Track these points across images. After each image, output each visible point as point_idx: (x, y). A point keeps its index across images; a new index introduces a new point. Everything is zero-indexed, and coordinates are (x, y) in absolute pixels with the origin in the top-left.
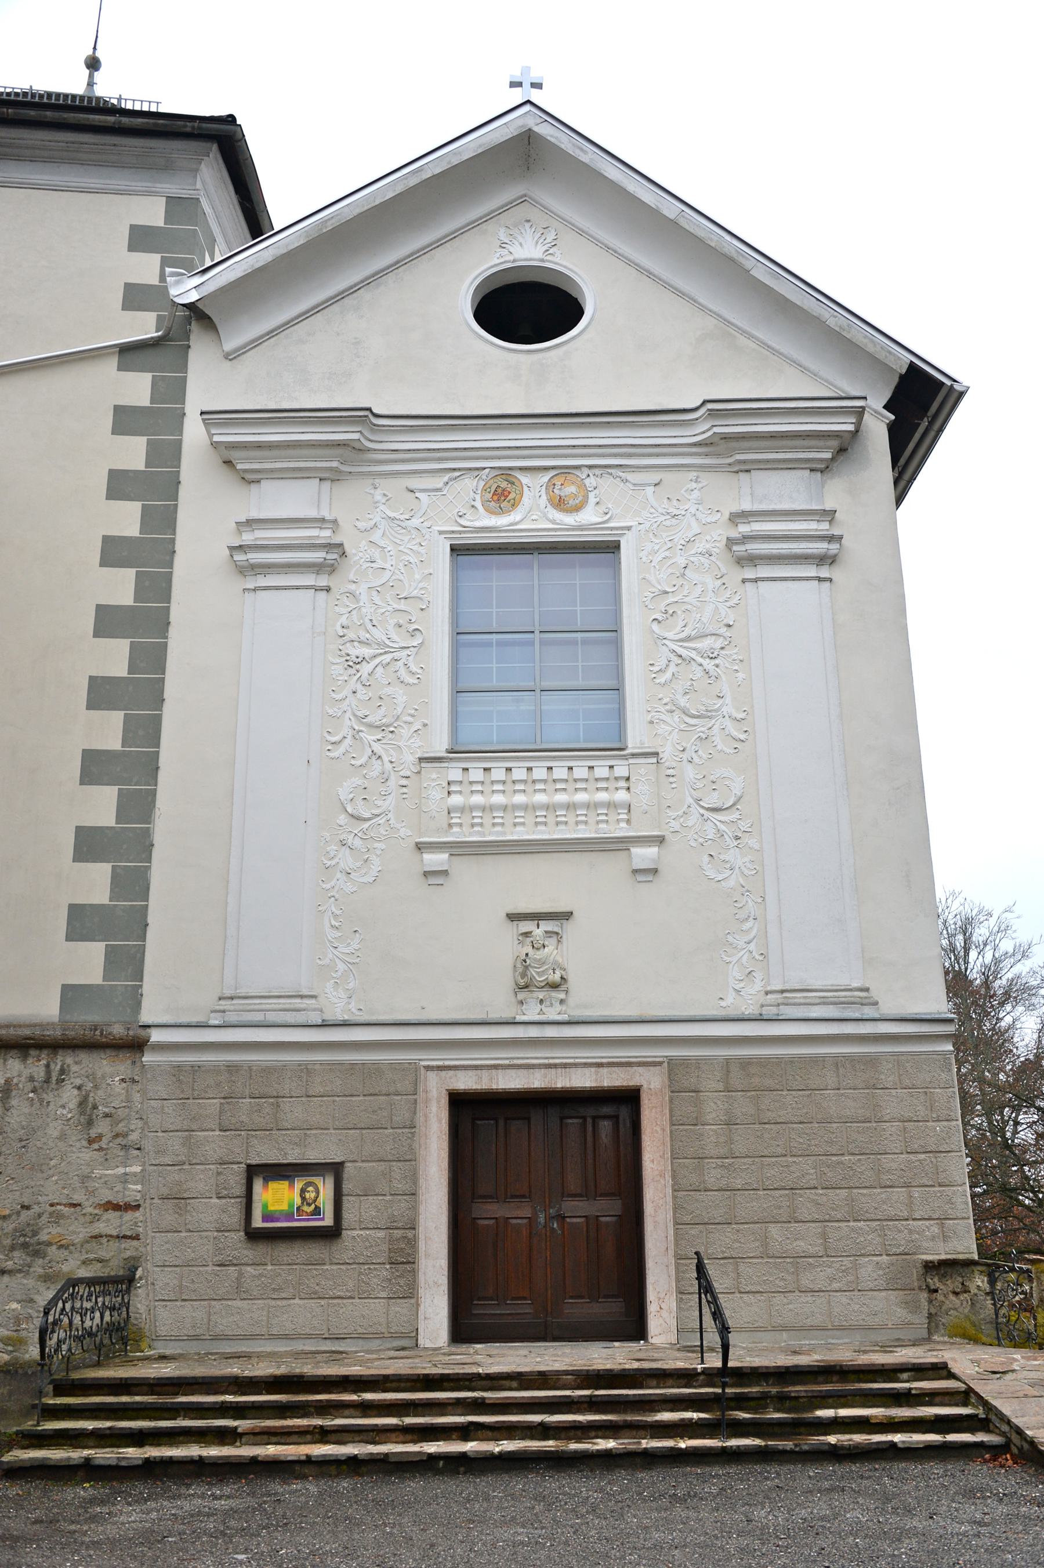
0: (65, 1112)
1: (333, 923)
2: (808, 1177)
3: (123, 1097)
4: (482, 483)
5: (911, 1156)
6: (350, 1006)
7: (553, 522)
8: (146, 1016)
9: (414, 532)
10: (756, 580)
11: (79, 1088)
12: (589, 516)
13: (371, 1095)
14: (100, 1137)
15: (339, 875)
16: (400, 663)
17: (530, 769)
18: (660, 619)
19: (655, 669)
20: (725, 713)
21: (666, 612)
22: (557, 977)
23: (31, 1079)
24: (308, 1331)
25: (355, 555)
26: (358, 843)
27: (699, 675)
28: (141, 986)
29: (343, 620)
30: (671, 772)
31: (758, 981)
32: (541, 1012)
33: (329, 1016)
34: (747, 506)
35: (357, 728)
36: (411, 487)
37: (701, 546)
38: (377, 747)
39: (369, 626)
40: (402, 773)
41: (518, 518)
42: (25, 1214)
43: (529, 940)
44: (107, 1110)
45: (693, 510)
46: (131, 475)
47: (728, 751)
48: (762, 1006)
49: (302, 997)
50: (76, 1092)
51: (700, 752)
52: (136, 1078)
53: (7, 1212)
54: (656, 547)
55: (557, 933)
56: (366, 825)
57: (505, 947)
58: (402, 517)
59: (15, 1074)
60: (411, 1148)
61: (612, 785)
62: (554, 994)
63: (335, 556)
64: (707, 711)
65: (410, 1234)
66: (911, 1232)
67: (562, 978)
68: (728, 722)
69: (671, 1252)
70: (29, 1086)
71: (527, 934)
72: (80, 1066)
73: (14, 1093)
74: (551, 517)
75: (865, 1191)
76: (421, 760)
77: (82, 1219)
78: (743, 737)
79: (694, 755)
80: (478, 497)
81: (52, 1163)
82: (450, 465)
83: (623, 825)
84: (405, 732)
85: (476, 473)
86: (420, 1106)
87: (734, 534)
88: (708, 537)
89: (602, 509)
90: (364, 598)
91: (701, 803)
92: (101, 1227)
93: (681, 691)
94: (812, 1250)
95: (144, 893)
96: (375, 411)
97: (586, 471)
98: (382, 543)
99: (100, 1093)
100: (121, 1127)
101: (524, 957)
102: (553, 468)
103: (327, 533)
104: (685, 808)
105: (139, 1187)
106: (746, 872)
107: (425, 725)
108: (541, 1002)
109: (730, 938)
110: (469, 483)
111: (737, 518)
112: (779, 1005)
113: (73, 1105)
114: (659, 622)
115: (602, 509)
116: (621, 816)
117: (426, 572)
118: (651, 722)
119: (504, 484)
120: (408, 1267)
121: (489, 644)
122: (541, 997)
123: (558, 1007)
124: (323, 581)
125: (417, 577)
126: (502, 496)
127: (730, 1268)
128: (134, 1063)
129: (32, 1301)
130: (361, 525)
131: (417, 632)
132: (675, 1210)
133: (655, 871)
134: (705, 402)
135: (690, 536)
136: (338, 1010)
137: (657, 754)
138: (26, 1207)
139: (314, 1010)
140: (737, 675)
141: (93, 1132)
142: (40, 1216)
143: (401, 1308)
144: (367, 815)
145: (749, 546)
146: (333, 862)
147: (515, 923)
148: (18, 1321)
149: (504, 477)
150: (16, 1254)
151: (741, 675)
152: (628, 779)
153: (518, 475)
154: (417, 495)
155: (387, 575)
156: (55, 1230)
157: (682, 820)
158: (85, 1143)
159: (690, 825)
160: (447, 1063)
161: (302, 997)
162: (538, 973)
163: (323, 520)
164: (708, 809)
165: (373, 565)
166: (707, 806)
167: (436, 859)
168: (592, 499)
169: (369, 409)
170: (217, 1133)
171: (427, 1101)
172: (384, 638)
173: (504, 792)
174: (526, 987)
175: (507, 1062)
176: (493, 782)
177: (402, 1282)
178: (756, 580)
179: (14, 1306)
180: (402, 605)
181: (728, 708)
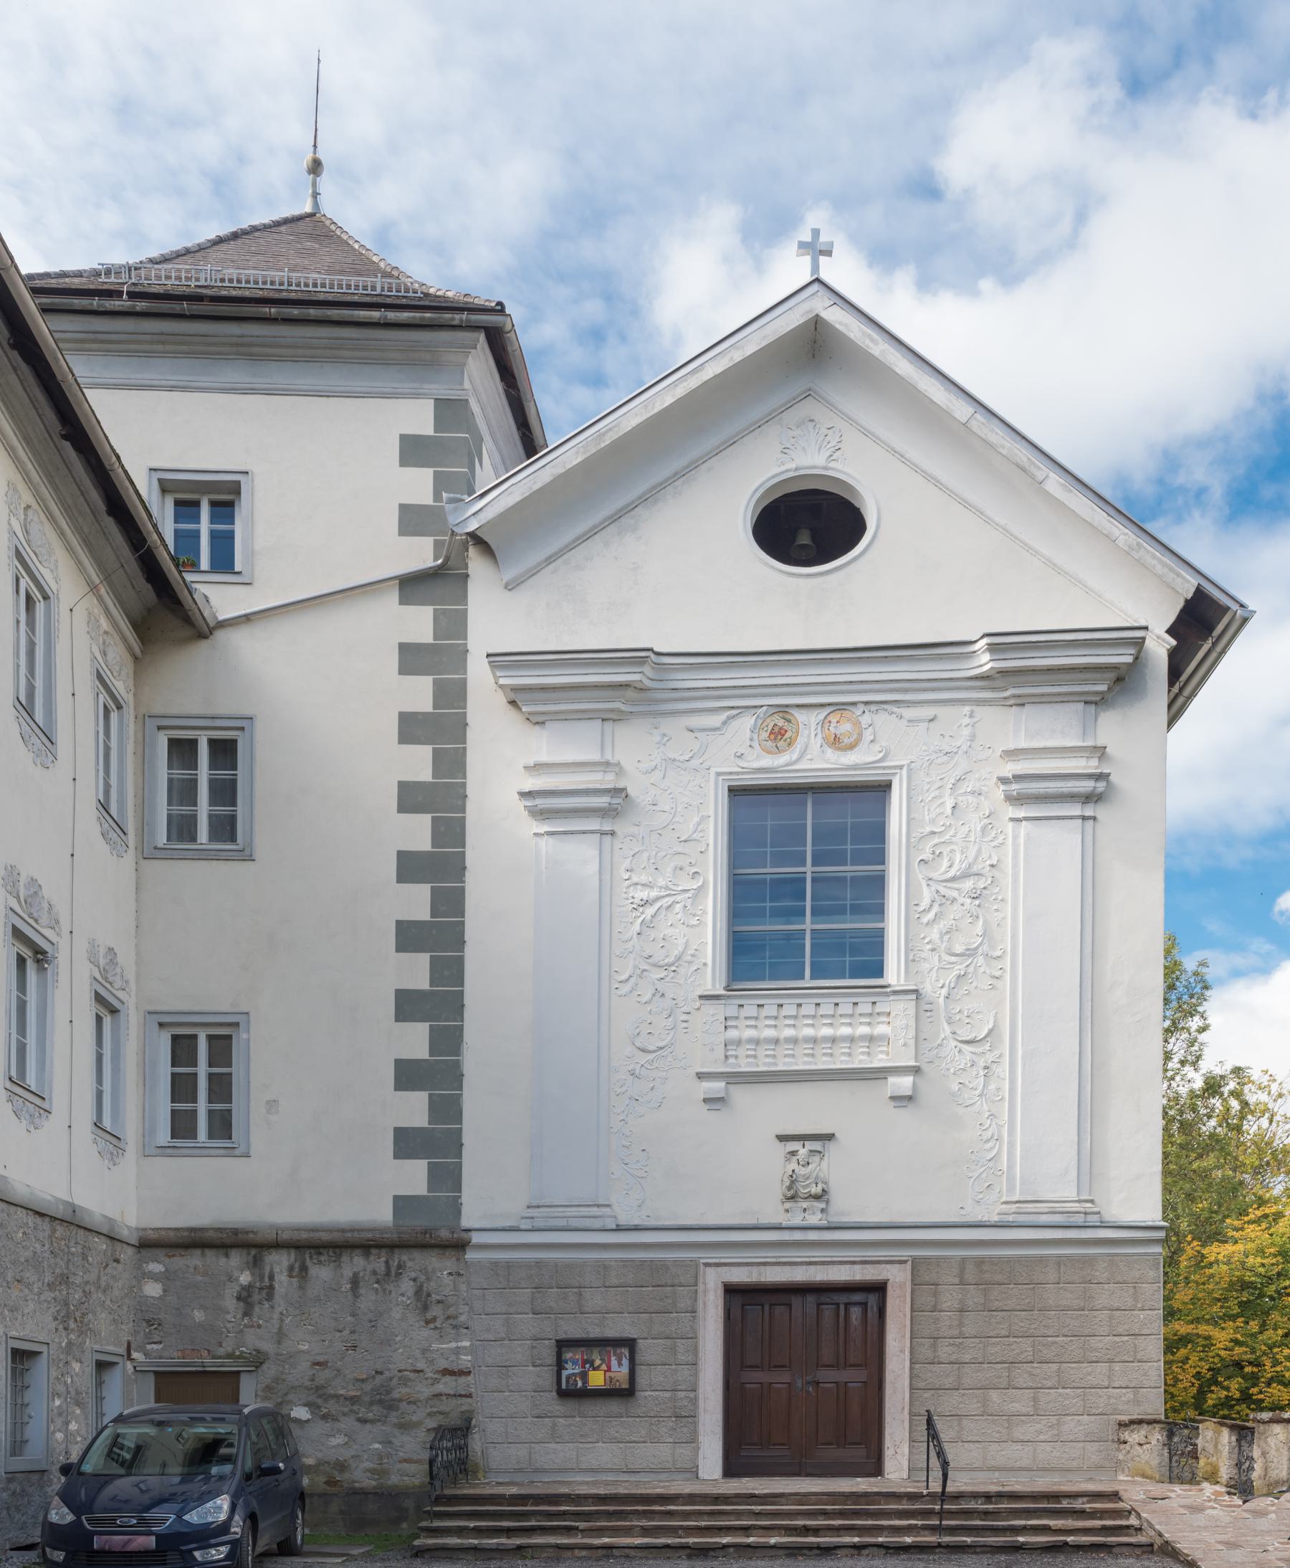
5: (1117, 1339)
8: (465, 1223)
11: (414, 1280)
14: (434, 1319)
17: (799, 1005)
23: (374, 1273)
38: (660, 986)
42: (378, 1378)
43: (795, 1158)
49: (598, 1206)
53: (365, 1376)
56: (651, 1056)
60: (694, 1330)
65: (692, 1395)
66: (1109, 1397)
69: (907, 1410)
70: (373, 1278)
71: (793, 1153)
72: (415, 1261)
76: (701, 997)
81: (398, 1339)
86: (700, 1295)
92: (440, 1388)
94: (1024, 1410)
95: (458, 1117)
99: (432, 1284)
100: (451, 1311)
105: (469, 1358)
113: (411, 1292)
123: (819, 1215)
127: (955, 1423)
128: (458, 1260)
129: (390, 1442)
132: (911, 1378)
138: (381, 1373)
141: (429, 1315)
142: (391, 1379)
144: (652, 1048)
146: (623, 1089)
148: (381, 1458)
150: (375, 1408)
156: (404, 1390)
158: (423, 1323)
160: (723, 1261)
161: (598, 1206)
167: (717, 1087)
171: (705, 1291)
177: (685, 1430)
179: (377, 1446)
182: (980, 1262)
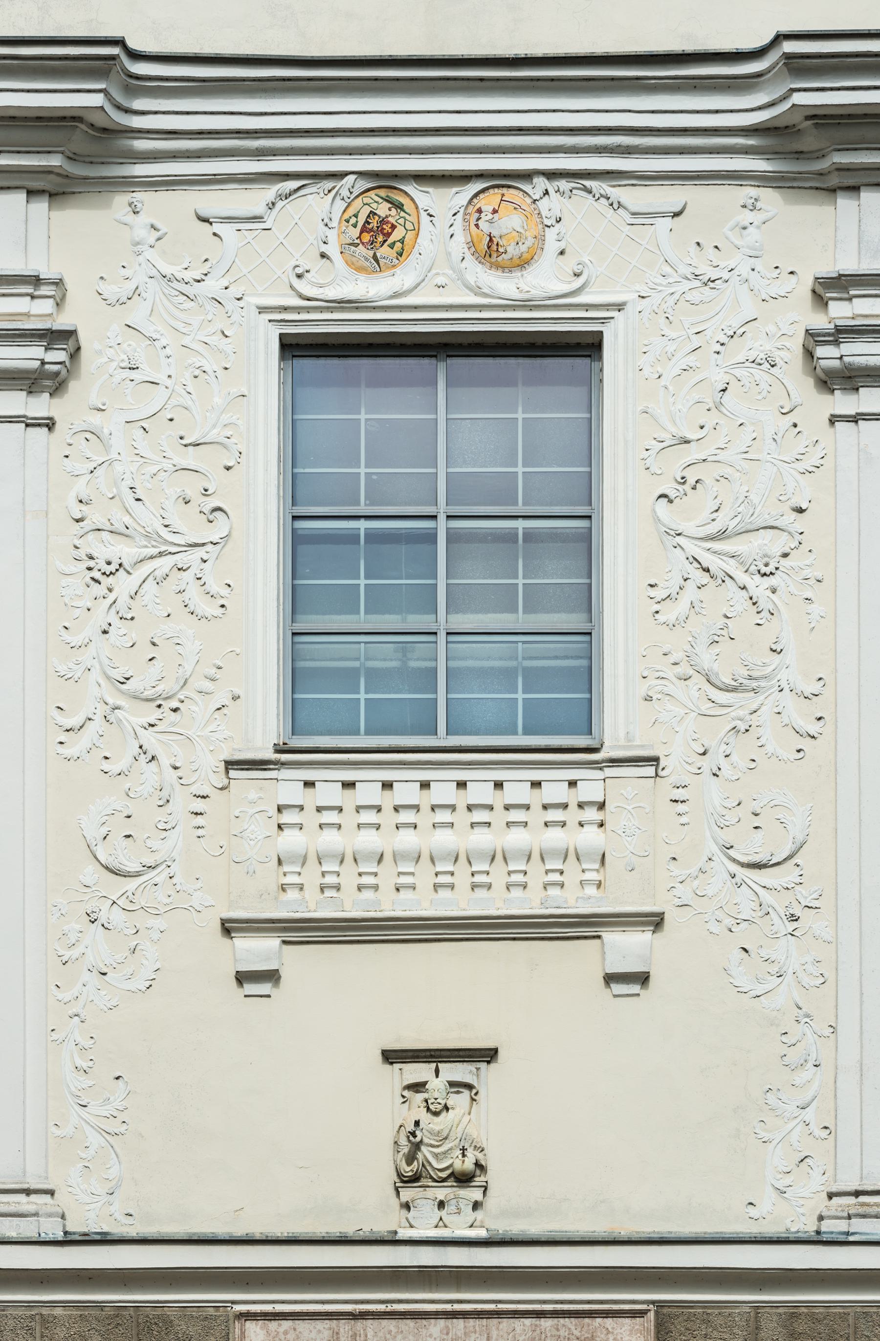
1: (79, 1063)
4: (340, 205)
6: (112, 1209)
7: (477, 291)
9: (211, 306)
10: (855, 419)
12: (544, 280)
15: (86, 976)
16: (188, 576)
17: (425, 785)
18: (672, 494)
19: (659, 593)
20: (784, 684)
21: (683, 481)
22: (469, 1165)
25: (99, 353)
26: (116, 917)
27: (739, 608)
29: (81, 488)
30: (679, 794)
31: (816, 1174)
32: (441, 1223)
33: (76, 1226)
34: (849, 265)
35: (110, 701)
36: (204, 213)
37: (757, 345)
38: (149, 738)
39: (129, 498)
41: (408, 284)
43: (420, 1097)
45: (744, 270)
47: (784, 755)
48: (821, 1218)
49: (28, 1192)
51: (734, 758)
54: (671, 348)
55: (469, 1087)
56: (131, 884)
57: (381, 1106)
58: (188, 276)
61: (573, 815)
62: (463, 1192)
63: (61, 356)
64: (750, 678)
67: (478, 1165)
68: (788, 701)
71: (418, 1087)
74: (471, 280)
76: (230, 765)
78: (813, 728)
79: (723, 763)
80: (332, 236)
82: (279, 162)
83: (591, 890)
84: (198, 710)
85: (328, 184)
87: (821, 322)
88: (771, 328)
89: (569, 264)
90: (118, 444)
91: (731, 852)
93: (704, 640)
96: (132, 44)
97: (541, 183)
98: (150, 331)
101: (411, 1127)
102: (481, 175)
103: (45, 306)
104: (701, 862)
106: (806, 980)
107: (235, 698)
108: (441, 1205)
109: (771, 1098)
110: (316, 204)
111: (832, 287)
112: (849, 1217)
114: (671, 501)
115: (569, 264)
116: (588, 876)
117: (235, 391)
118: (648, 699)
119: (383, 209)
121: (352, 538)
122: (441, 1197)
123: (469, 1215)
124: (39, 406)
125: (217, 400)
126: (376, 236)
130: (111, 290)
131: (218, 514)
133: (643, 979)
134: (779, 38)
135: (736, 324)
136: (92, 1215)
137: (656, 759)
139: (50, 1215)
140: (810, 608)
145: (846, 348)
146: (75, 953)
147: (397, 1066)
149: (383, 193)
151: (816, 609)
152: (602, 806)
153: (411, 188)
154: (217, 228)
155: (159, 397)
157: (696, 883)
159: (710, 893)
160: (279, 1308)
161: (28, 1192)
162: (436, 1156)
163: (36, 281)
164: (743, 865)
165: (133, 374)
166: (744, 859)
167: (258, 950)
168: (552, 246)
169: (119, 42)
172: (158, 526)
173: (378, 827)
174: (415, 1178)
175: (381, 1307)
176: (358, 809)
178: (855, 419)
180: (190, 458)
181: (792, 671)
182: (793, 1313)
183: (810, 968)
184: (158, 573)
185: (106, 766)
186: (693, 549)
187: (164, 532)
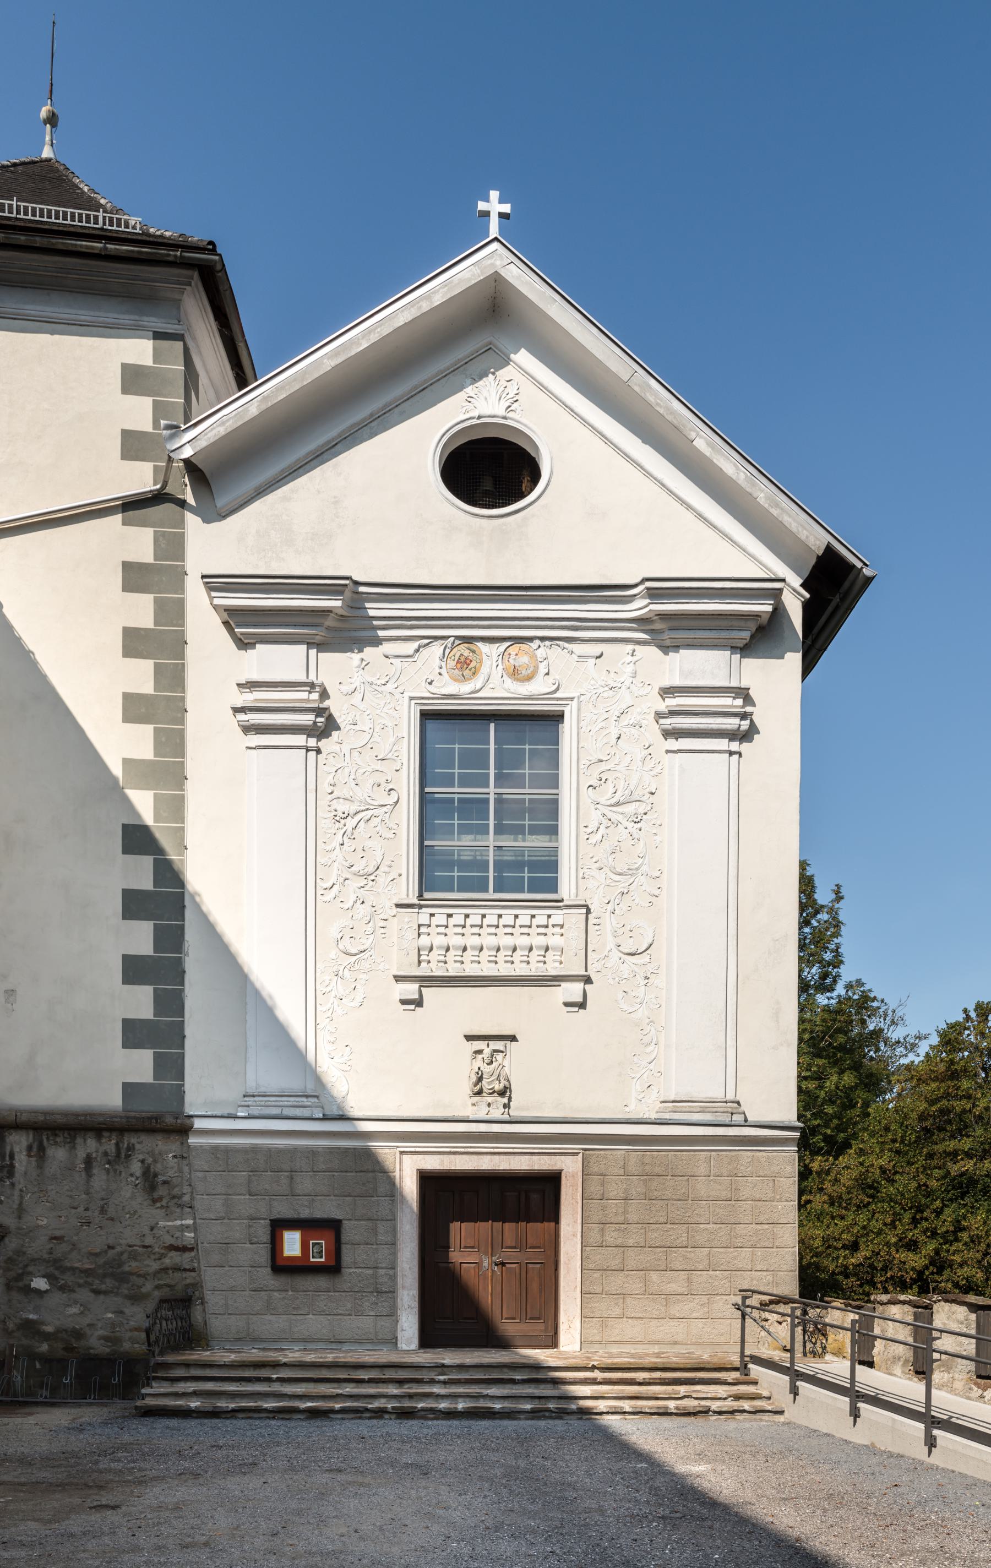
0: (133, 1179)
2: (681, 1239)
3: (176, 1169)
5: (758, 1226)
7: (508, 691)
8: (189, 1110)
9: (388, 696)
11: (143, 1161)
12: (538, 686)
13: (361, 1172)
19: (589, 830)
23: (106, 1154)
24: (319, 1336)
27: (624, 837)
28: (183, 1085)
36: (387, 654)
40: (382, 916)
41: (478, 687)
44: (164, 1178)
45: (627, 683)
46: (142, 632)
49: (307, 1096)
50: (139, 1164)
52: (185, 1155)
58: (379, 682)
59: (93, 1150)
65: (391, 1272)
71: (479, 1052)
72: (144, 1144)
73: (94, 1164)
75: (722, 1250)
76: (397, 906)
77: (153, 1257)
78: (657, 892)
94: (680, 1290)
95: (181, 1011)
97: (537, 642)
100: (176, 1191)
105: (192, 1235)
110: (436, 649)
111: (667, 692)
113: (138, 1173)
115: (550, 679)
119: (466, 653)
120: (390, 1295)
126: (466, 667)
128: (182, 1143)
141: (156, 1195)
143: (385, 1323)
144: (354, 951)
146: (328, 989)
149: (466, 645)
153: (480, 644)
154: (392, 660)
158: (149, 1202)
160: (418, 1150)
165: (354, 727)
168: (542, 669)
170: (247, 1197)
175: (463, 1150)
177: (385, 1304)
183: (654, 1000)
184: (365, 818)
185: (342, 905)
186: (606, 811)
187: (368, 799)
